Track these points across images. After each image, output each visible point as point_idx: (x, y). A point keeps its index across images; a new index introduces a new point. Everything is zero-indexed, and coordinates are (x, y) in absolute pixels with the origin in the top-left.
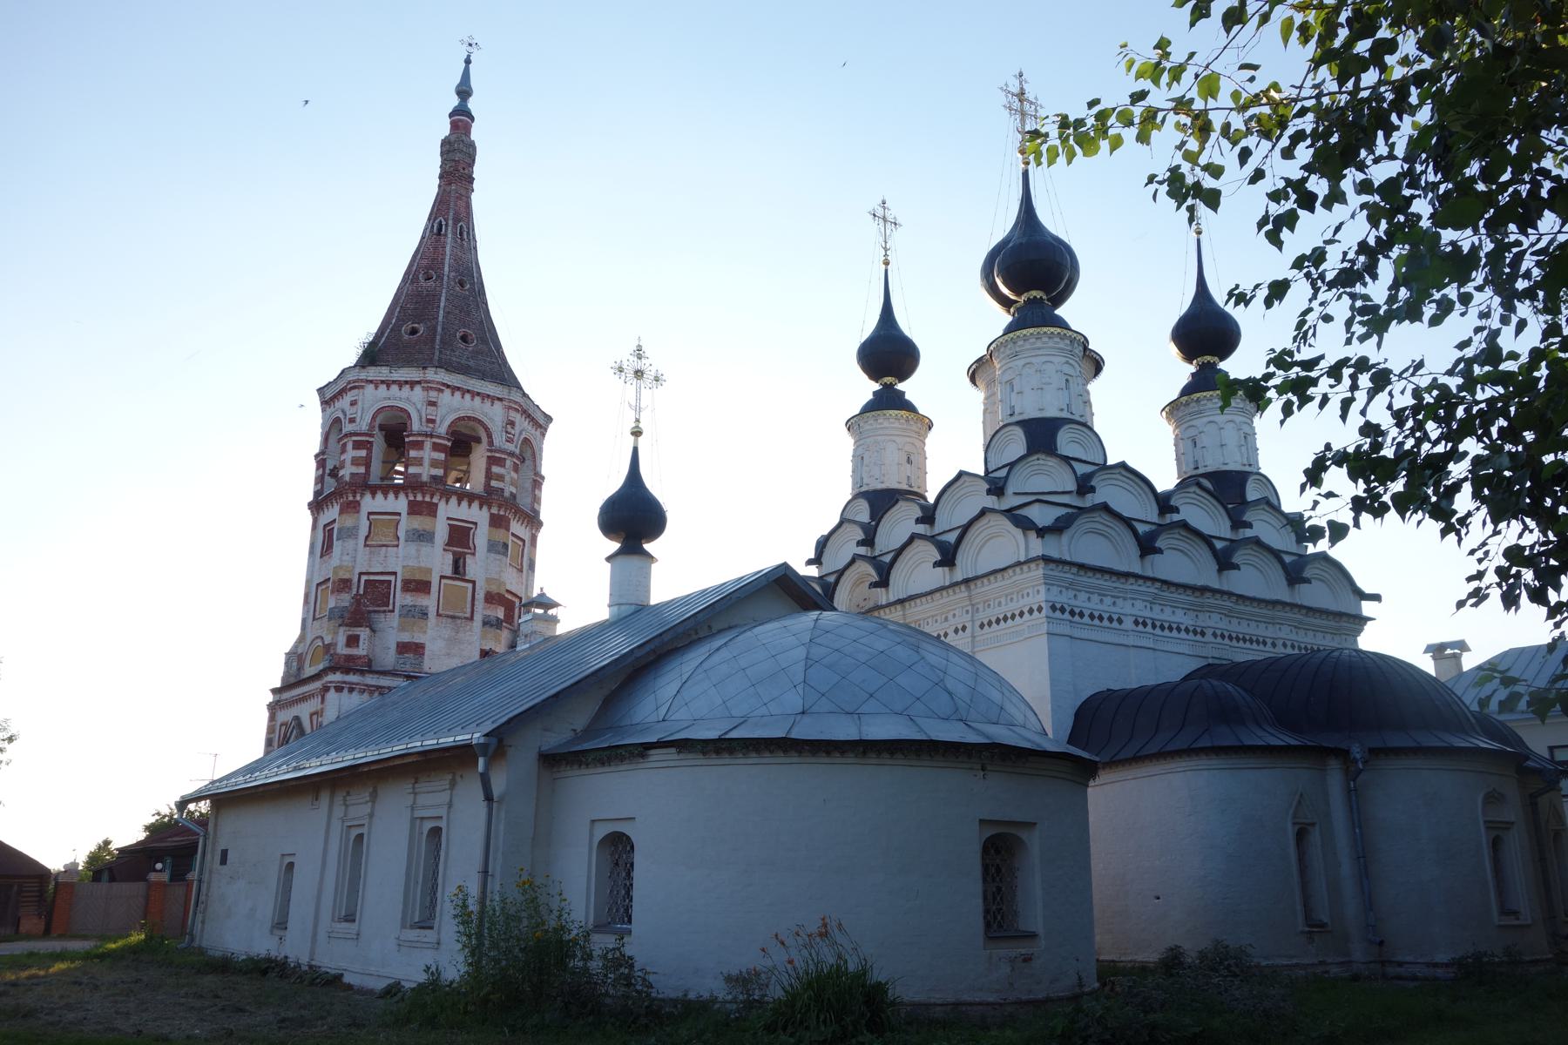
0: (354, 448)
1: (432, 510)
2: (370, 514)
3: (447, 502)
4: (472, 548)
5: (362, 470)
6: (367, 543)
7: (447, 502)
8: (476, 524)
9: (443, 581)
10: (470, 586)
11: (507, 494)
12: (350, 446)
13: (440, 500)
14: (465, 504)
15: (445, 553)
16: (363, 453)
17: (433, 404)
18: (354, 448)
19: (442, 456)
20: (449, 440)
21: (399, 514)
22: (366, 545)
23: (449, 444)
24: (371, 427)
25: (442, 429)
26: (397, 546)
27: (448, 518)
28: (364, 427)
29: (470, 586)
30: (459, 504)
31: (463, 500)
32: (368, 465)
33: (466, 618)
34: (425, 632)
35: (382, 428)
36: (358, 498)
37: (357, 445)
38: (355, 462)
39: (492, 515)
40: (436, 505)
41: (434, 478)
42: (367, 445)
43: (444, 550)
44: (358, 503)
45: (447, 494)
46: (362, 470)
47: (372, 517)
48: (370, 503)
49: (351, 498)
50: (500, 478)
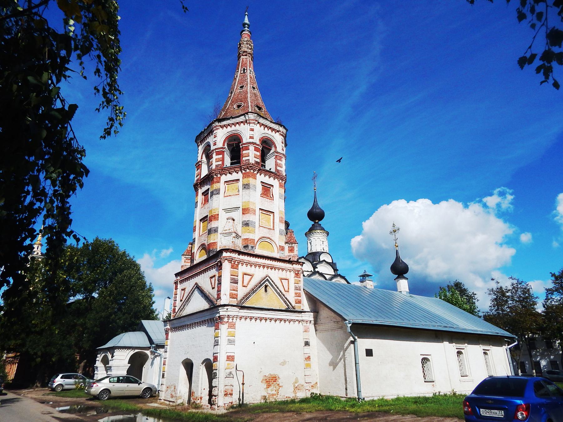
3: (260, 175)
4: (272, 197)
6: (225, 195)
7: (260, 175)
9: (261, 212)
12: (215, 153)
13: (257, 173)
16: (221, 156)
17: (252, 130)
24: (224, 145)
25: (257, 140)
26: (239, 194)
27: (261, 182)
28: (221, 146)
32: (223, 160)
35: (229, 145)
36: (219, 176)
37: (218, 154)
38: (217, 160)
39: (280, 183)
42: (222, 153)
43: (261, 196)
44: (220, 178)
46: (220, 163)
47: (225, 184)
48: (224, 178)
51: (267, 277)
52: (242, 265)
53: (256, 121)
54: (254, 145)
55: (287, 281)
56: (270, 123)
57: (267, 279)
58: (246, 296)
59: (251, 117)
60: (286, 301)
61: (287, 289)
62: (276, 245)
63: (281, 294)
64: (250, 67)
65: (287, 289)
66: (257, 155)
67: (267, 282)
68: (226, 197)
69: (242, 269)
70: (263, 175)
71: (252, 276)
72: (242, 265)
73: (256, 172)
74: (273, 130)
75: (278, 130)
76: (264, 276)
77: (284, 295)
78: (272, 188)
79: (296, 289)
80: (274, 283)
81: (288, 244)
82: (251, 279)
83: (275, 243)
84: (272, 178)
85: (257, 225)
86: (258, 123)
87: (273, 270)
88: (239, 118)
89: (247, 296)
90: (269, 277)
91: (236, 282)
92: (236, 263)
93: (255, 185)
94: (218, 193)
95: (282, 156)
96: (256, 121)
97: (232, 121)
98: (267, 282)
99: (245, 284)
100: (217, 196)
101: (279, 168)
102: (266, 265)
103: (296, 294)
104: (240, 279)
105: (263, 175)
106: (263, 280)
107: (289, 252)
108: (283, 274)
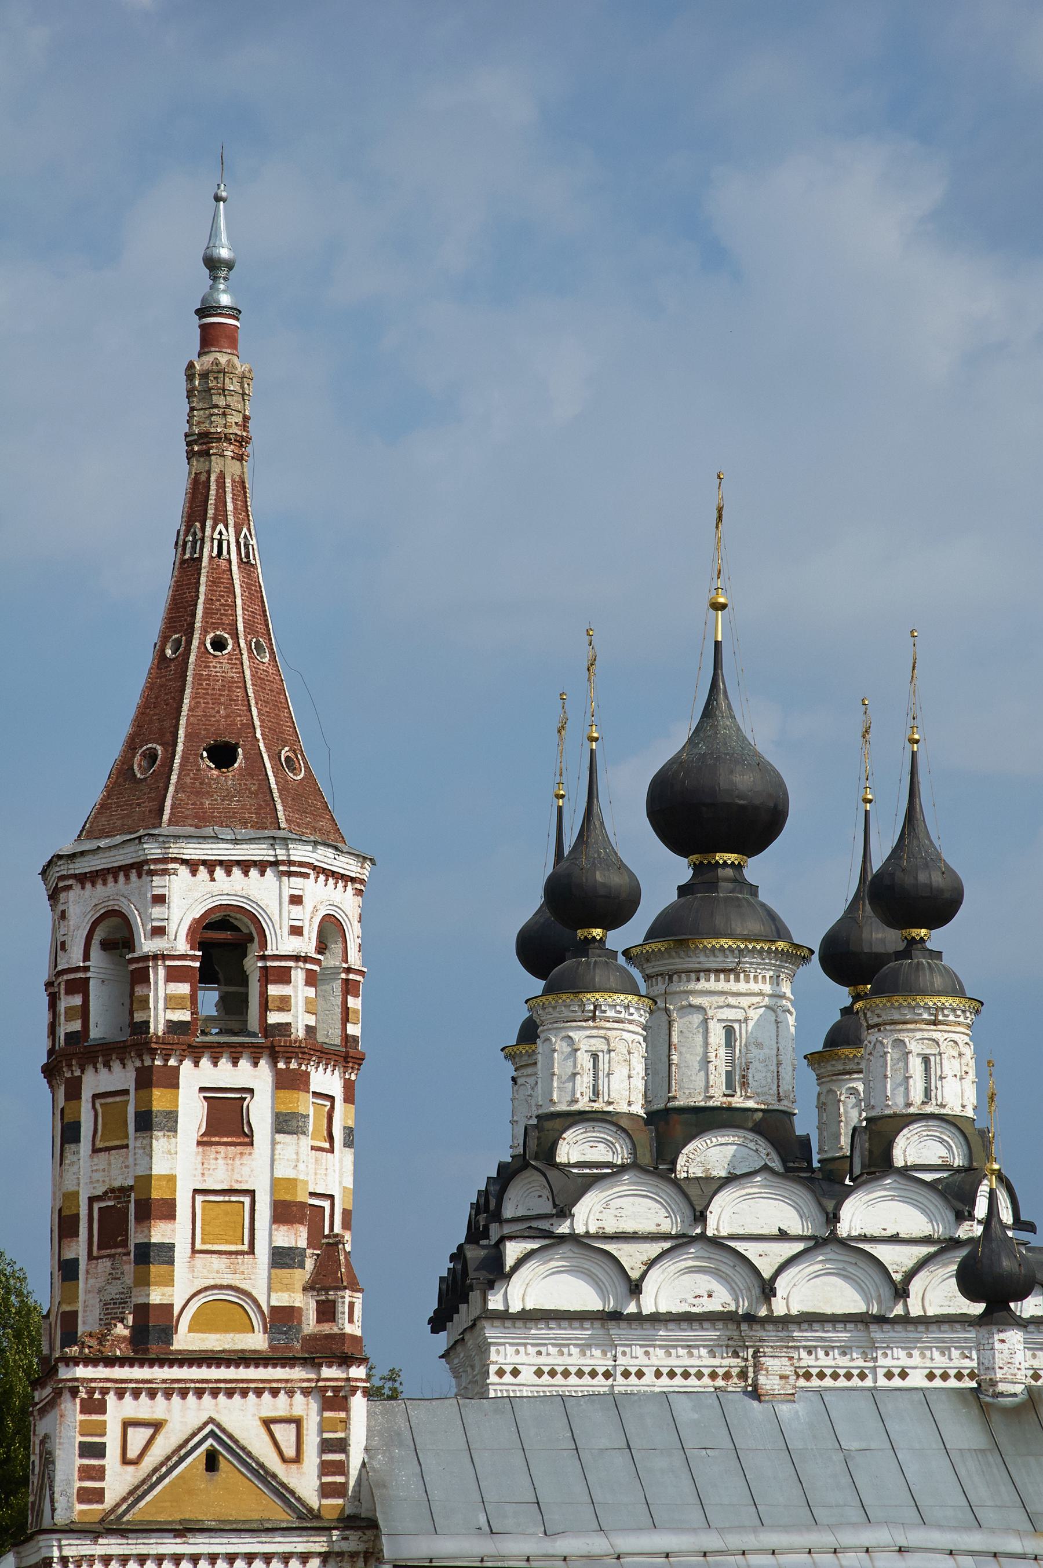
0: (67, 993)
1: (172, 1081)
2: (95, 1097)
5: (76, 1026)
6: (99, 1145)
7: (196, 1064)
8: (251, 1091)
9: (199, 1198)
10: (247, 1200)
11: (299, 1033)
14: (224, 1063)
15: (201, 1149)
16: (77, 1000)
18: (67, 993)
19: (183, 989)
20: (193, 958)
21: (126, 1092)
22: (95, 1151)
23: (198, 964)
24: (86, 957)
27: (202, 1089)
29: (247, 1200)
30: (215, 1064)
31: (200, 1058)
33: (242, 1253)
34: (169, 1281)
40: (177, 1068)
41: (173, 1027)
43: (199, 1143)
44: (79, 1079)
45: (195, 1053)
49: (68, 1075)
50: (284, 1005)
51: (206, 1424)
52: (120, 1394)
53: (175, 860)
54: (168, 963)
55: (294, 1426)
56: (232, 846)
57: (212, 1434)
58: (131, 1493)
59: (153, 851)
60: (283, 1493)
61: (290, 1452)
62: (259, 1306)
63: (264, 1475)
64: (214, 529)
65: (290, 1452)
66: (182, 997)
67: (210, 1441)
68: (100, 1150)
69: (117, 1410)
70: (205, 1062)
71: (157, 1426)
72: (120, 1394)
73: (172, 1062)
74: (246, 866)
75: (272, 859)
76: (204, 1419)
77: (274, 1476)
78: (248, 1096)
79: (326, 1446)
80: (236, 1441)
81: (315, 1293)
82: (152, 1438)
83: (255, 1301)
84: (244, 1063)
85: (182, 1253)
86: (184, 862)
87: (237, 1397)
88: (122, 851)
89: (136, 1494)
90: (219, 1426)
91: (97, 1450)
92: (97, 1396)
93: (171, 1112)
94: (77, 1140)
95: (291, 964)
96: (175, 860)
97: (104, 861)
98: (210, 1441)
99: (132, 1453)
100: (73, 1147)
101: (274, 1018)
102: (211, 1385)
103: (326, 1468)
104: (112, 1441)
105: (205, 1062)
106: (194, 1435)
107: (319, 1321)
108: (280, 1406)
